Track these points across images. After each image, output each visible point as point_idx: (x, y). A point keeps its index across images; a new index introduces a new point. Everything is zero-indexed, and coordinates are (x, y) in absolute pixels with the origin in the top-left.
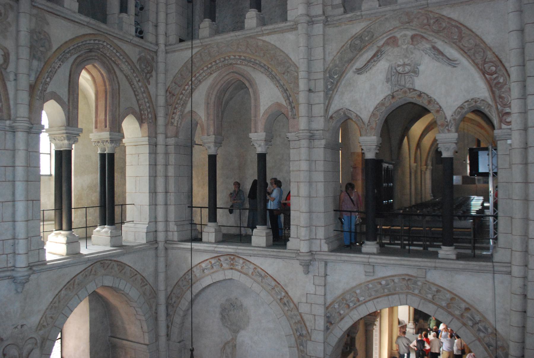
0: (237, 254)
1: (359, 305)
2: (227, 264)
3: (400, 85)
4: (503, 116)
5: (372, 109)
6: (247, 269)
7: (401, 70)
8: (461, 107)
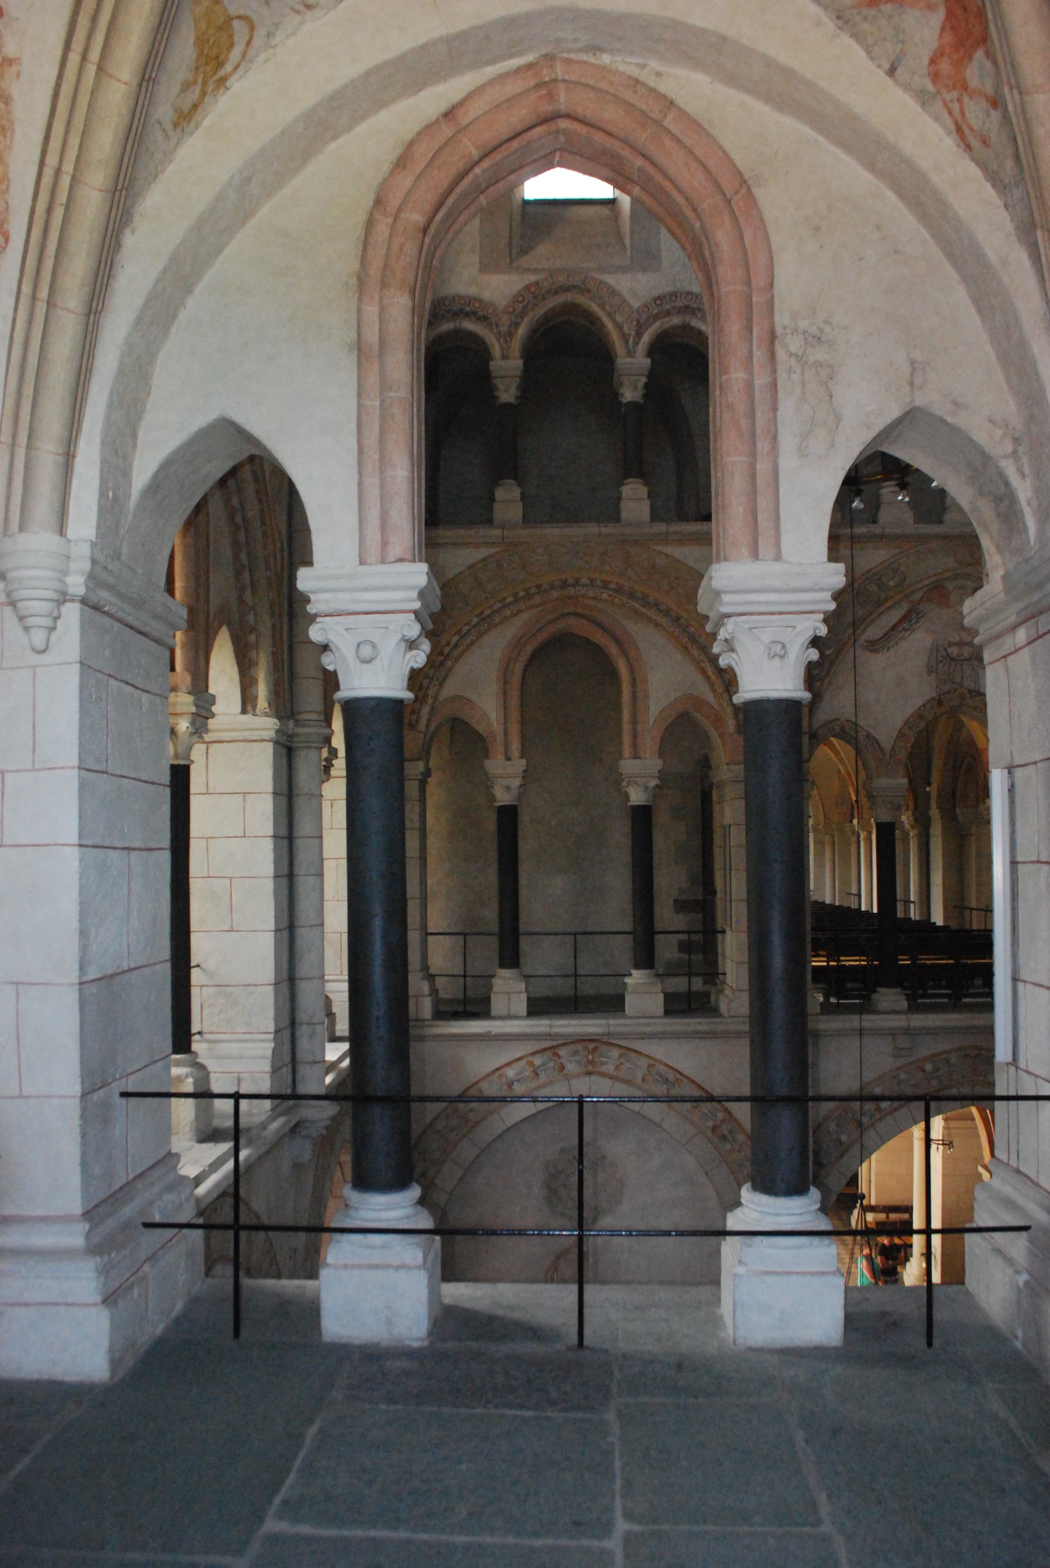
0: (605, 1039)
1: (880, 1119)
2: (579, 1062)
3: (953, 683)
5: (899, 723)
6: (630, 1068)
7: (956, 652)
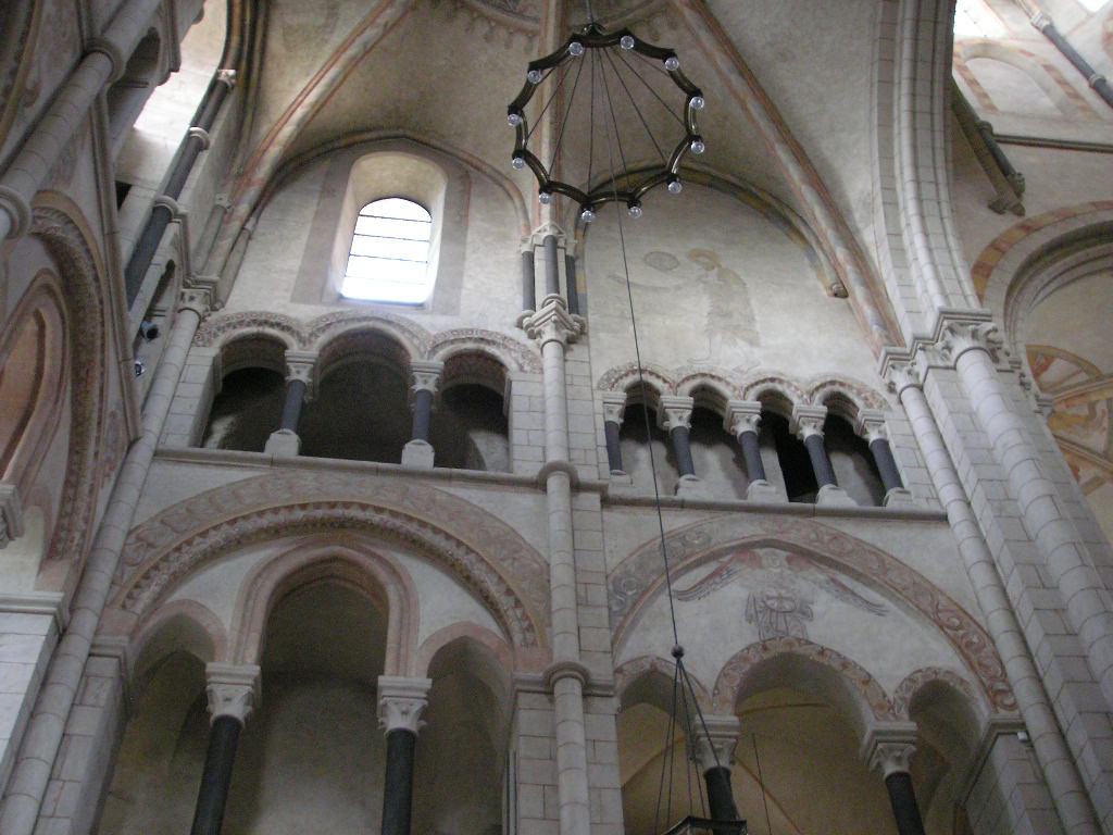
4: (995, 696)
5: (722, 665)
7: (776, 605)
8: (910, 679)
